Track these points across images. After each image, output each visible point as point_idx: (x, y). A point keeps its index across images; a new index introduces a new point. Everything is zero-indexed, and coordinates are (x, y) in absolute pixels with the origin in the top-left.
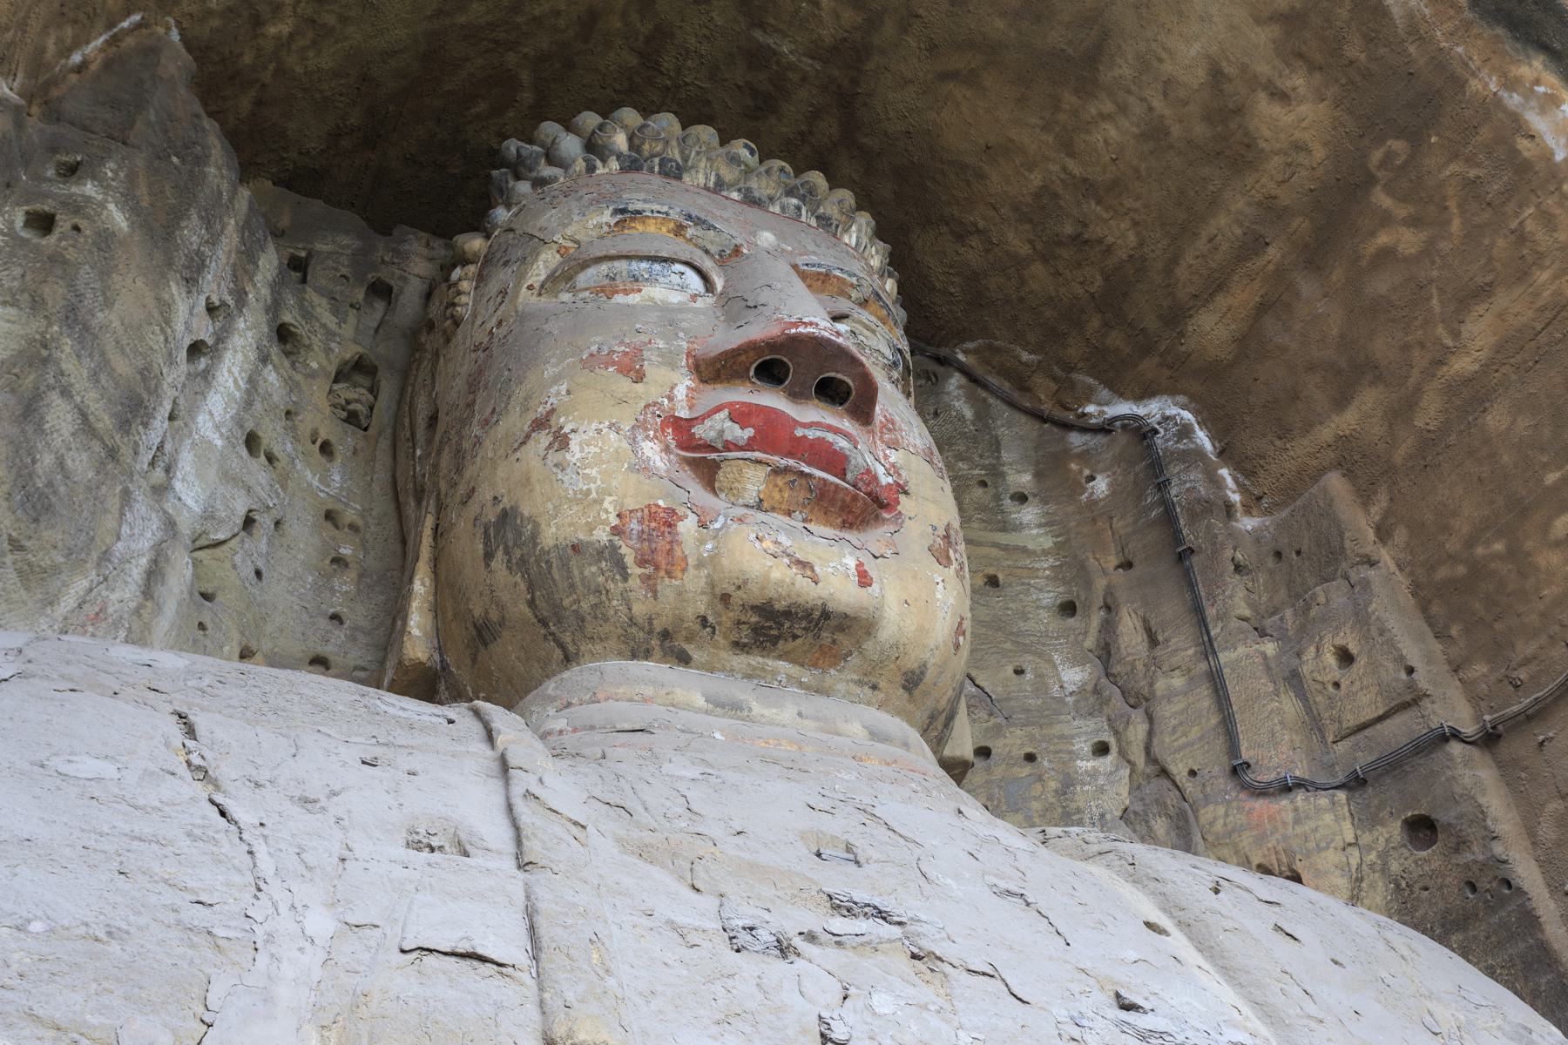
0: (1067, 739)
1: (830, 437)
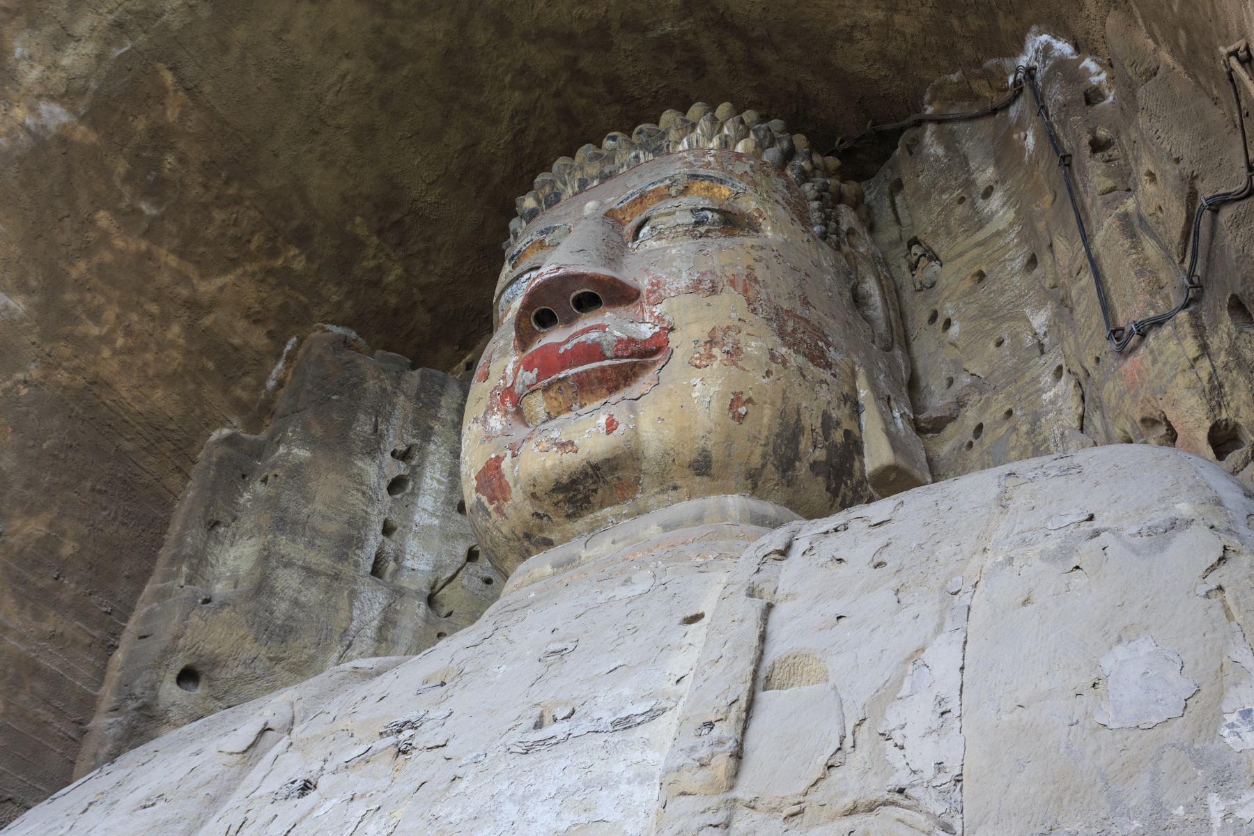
0: (1035, 380)
1: (583, 338)
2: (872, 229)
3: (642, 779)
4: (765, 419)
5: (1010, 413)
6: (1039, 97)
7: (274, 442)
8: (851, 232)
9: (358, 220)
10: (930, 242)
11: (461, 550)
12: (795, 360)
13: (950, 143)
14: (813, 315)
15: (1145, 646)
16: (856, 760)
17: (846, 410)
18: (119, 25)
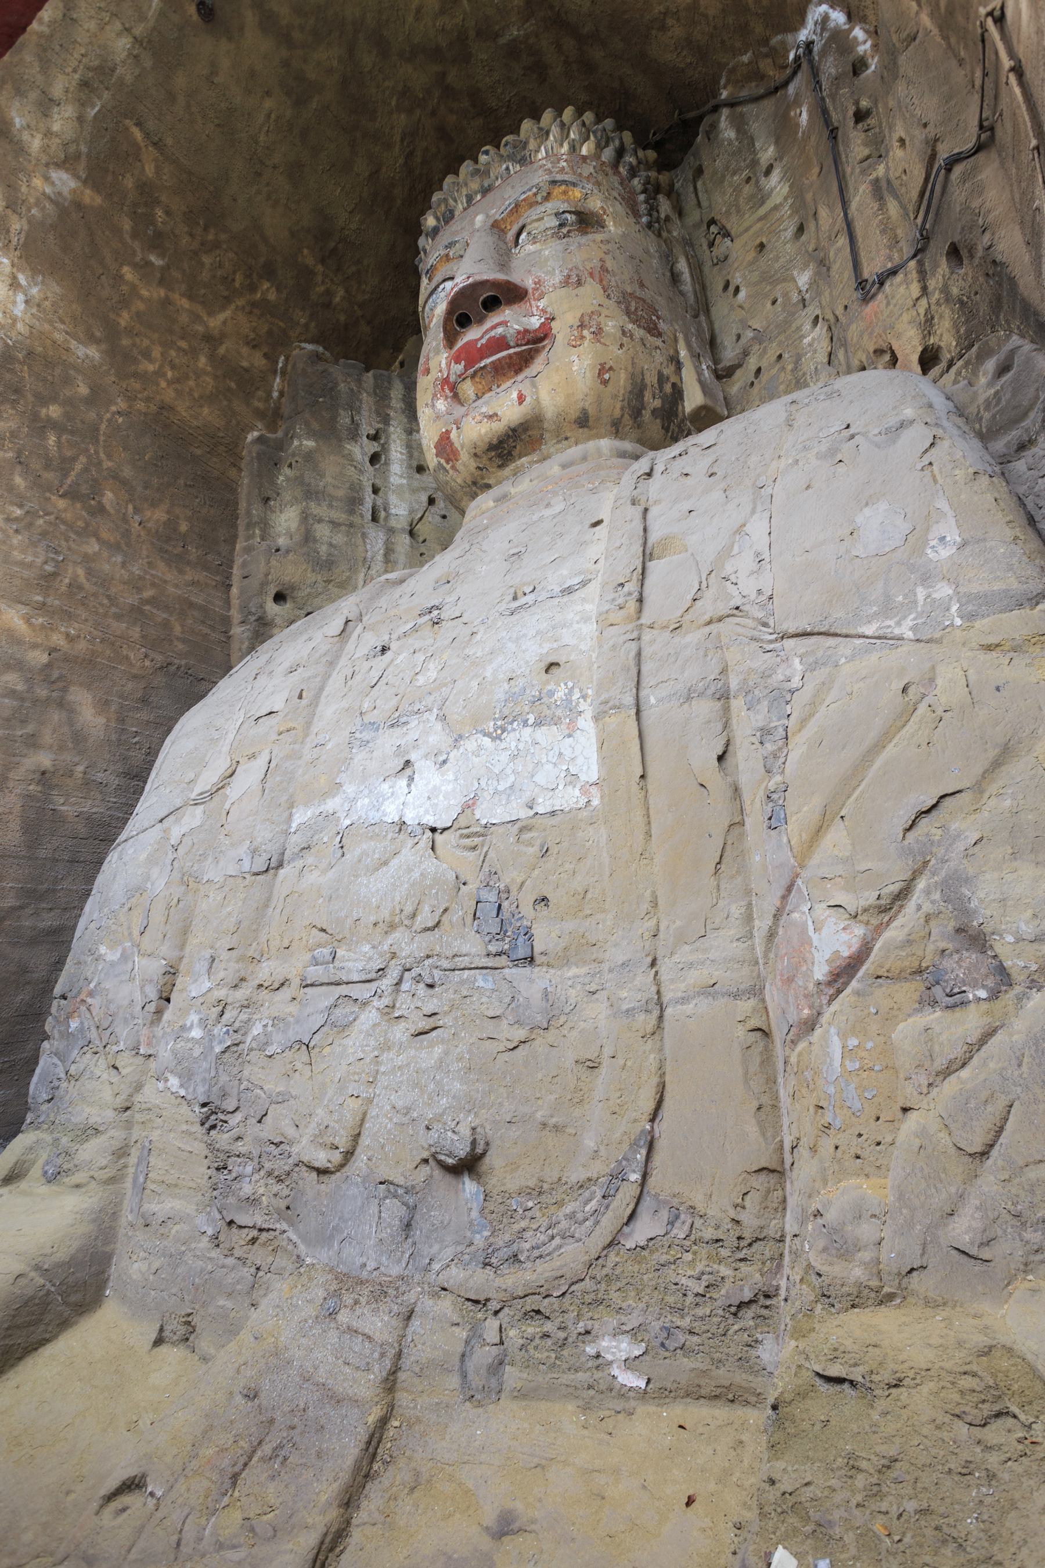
0: (799, 329)
1: (493, 333)
2: (681, 214)
3: (586, 620)
4: (621, 381)
5: (780, 356)
6: (815, 73)
7: (289, 436)
8: (667, 219)
9: (305, 251)
10: (724, 222)
11: (424, 499)
12: (639, 333)
13: (740, 124)
14: (647, 294)
15: (883, 506)
16: (709, 595)
17: (672, 368)
18: (84, 84)
